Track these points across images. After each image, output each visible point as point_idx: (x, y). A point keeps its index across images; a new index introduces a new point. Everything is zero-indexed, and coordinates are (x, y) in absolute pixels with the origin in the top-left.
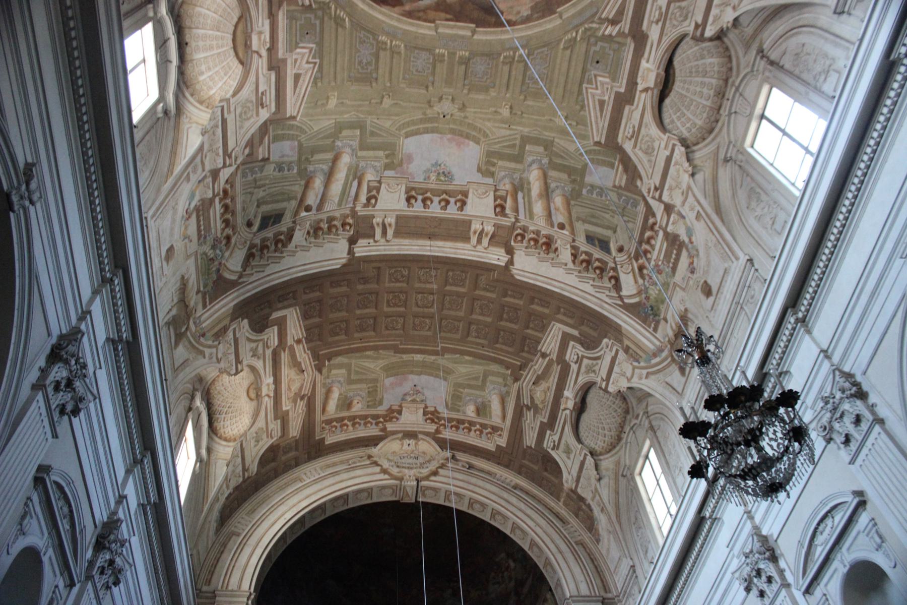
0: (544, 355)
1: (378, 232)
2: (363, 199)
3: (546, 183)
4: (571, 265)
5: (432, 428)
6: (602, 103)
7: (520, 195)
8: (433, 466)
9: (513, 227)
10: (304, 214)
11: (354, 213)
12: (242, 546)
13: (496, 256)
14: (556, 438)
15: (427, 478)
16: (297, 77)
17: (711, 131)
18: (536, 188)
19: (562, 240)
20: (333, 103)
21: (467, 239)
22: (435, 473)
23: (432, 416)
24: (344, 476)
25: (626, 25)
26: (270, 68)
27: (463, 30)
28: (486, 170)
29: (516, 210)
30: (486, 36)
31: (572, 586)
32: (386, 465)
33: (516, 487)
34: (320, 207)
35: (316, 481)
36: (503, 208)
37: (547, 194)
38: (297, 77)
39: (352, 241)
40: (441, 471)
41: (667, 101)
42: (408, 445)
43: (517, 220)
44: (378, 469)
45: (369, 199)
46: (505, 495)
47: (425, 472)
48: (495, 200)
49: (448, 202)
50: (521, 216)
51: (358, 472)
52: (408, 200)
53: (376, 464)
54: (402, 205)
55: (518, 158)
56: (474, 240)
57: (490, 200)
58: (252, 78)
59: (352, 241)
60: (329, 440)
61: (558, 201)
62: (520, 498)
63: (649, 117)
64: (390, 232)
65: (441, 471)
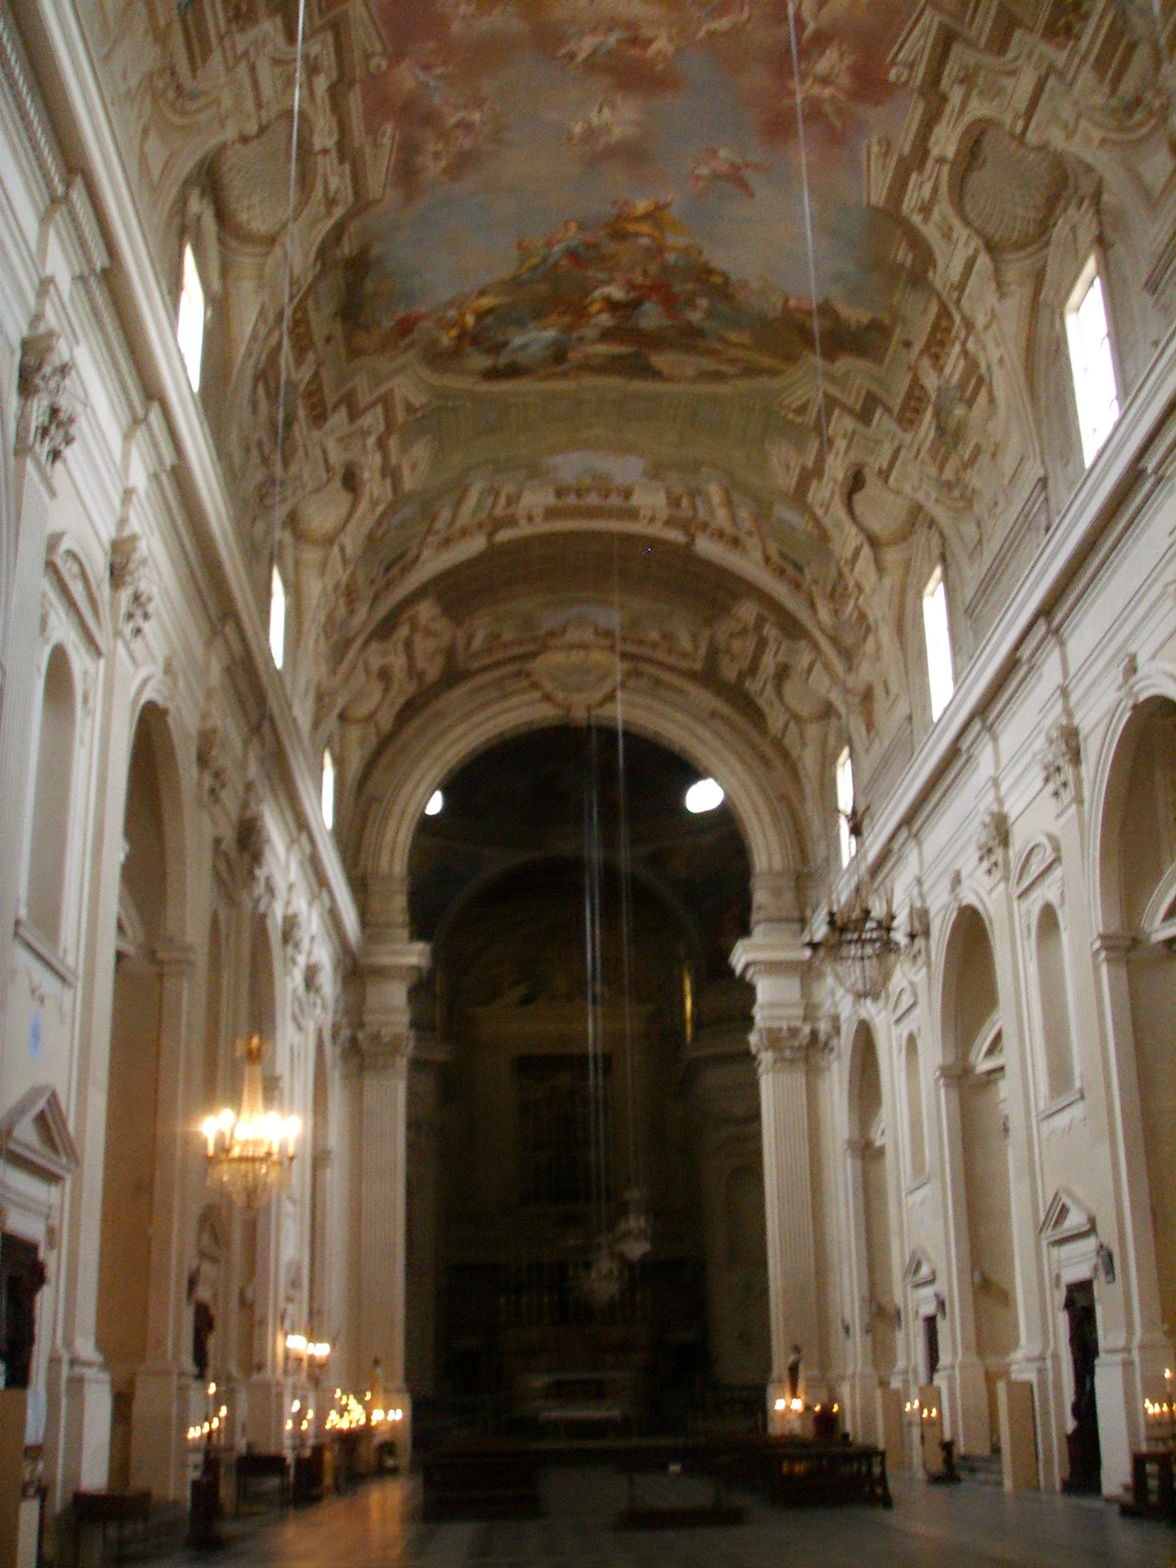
1: (523, 522)
4: (761, 562)
8: (606, 687)
12: (386, 817)
13: (675, 536)
15: (601, 704)
17: (904, 539)
19: (752, 543)
23: (608, 634)
24: (496, 708)
25: (811, 417)
26: (384, 476)
27: (615, 382)
28: (656, 472)
29: (695, 508)
31: (764, 858)
32: (549, 686)
33: (714, 714)
35: (460, 720)
37: (729, 503)
38: (413, 467)
39: (491, 535)
41: (858, 498)
42: (575, 657)
43: (695, 517)
44: (537, 695)
45: (509, 504)
47: (598, 695)
48: (668, 497)
49: (607, 496)
51: (515, 701)
52: (559, 494)
54: (550, 499)
56: (646, 521)
60: (475, 665)
61: (744, 514)
62: (717, 734)
64: (538, 520)
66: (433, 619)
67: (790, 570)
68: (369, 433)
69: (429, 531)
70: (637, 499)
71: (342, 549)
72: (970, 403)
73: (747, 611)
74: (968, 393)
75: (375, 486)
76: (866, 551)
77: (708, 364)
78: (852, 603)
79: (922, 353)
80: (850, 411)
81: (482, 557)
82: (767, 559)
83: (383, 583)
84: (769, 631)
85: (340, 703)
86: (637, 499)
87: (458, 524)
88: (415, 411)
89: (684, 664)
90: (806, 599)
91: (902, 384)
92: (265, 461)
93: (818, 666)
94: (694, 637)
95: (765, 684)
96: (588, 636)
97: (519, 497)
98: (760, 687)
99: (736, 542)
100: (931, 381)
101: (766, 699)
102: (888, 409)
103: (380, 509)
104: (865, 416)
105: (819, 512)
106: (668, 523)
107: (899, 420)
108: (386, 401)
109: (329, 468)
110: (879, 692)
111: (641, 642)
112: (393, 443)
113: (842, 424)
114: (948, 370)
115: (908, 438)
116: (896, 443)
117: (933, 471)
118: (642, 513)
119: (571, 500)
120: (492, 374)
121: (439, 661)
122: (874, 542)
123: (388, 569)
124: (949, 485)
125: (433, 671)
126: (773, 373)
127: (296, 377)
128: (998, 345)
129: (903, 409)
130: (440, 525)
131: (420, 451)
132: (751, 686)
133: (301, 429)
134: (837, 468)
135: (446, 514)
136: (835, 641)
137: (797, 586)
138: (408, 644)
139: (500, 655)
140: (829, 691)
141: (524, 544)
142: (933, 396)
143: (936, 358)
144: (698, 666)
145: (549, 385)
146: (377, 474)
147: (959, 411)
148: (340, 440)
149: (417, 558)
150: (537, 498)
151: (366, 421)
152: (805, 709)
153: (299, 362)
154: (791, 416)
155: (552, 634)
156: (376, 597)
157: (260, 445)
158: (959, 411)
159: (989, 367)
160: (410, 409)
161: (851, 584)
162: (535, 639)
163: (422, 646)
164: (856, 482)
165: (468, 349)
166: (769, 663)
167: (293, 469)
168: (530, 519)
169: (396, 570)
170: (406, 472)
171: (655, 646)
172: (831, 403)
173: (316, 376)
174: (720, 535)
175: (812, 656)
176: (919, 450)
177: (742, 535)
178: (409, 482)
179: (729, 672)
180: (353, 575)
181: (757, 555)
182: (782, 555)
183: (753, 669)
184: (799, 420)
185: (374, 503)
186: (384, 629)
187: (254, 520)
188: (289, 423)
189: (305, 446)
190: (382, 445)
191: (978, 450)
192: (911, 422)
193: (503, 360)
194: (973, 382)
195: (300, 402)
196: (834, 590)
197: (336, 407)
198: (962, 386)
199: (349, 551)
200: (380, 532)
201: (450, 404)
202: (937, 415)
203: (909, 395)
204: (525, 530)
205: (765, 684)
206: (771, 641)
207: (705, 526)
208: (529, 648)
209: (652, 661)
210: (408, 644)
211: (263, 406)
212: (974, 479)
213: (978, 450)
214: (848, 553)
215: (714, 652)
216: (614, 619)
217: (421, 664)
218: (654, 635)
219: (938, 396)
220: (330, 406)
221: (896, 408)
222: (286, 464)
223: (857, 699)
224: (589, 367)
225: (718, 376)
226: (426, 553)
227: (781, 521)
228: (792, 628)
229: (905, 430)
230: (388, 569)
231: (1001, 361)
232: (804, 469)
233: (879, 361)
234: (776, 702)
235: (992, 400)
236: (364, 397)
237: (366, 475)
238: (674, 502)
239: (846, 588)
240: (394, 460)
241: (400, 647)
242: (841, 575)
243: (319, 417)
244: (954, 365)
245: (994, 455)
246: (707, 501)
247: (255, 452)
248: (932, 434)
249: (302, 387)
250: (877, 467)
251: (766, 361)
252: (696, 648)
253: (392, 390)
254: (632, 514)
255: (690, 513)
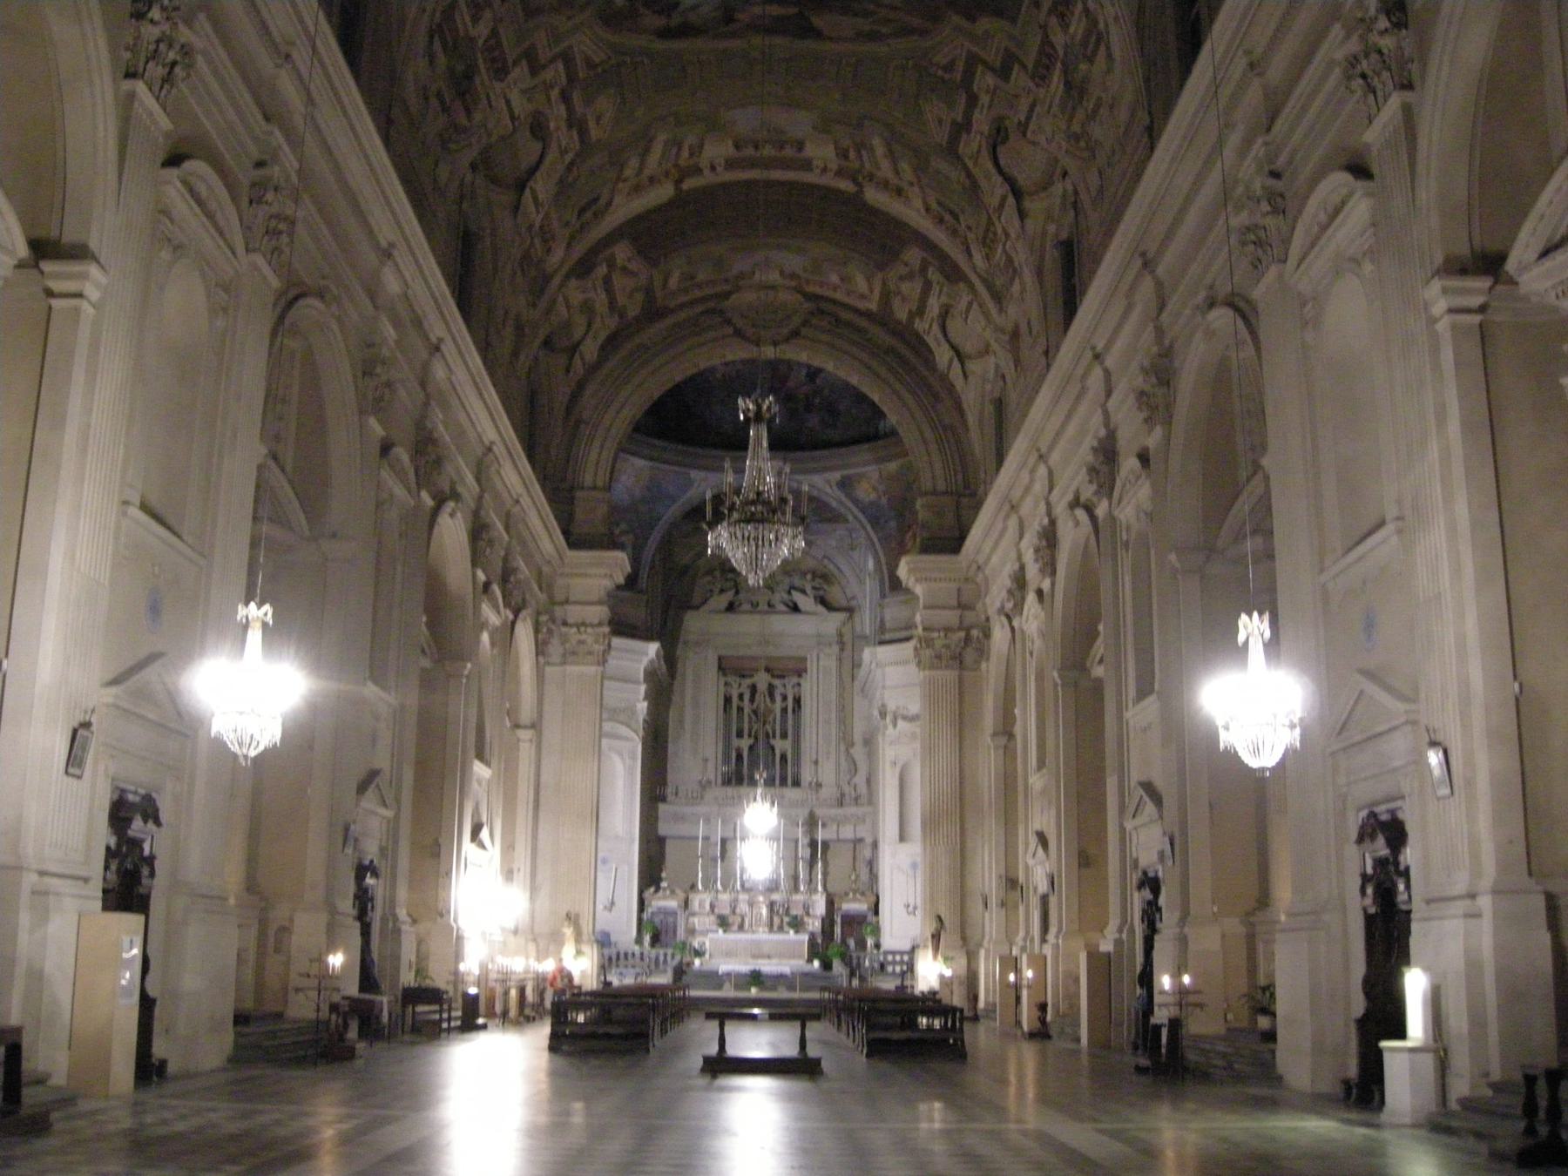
0: (906, 265)
1: (706, 172)
2: (685, 153)
3: (890, 150)
4: (923, 211)
5: (793, 284)
6: (940, 121)
7: (864, 152)
9: (859, 171)
10: (621, 185)
11: (676, 165)
14: (927, 326)
16: (598, 119)
17: (1045, 189)
18: (880, 150)
20: (639, 113)
21: (812, 170)
22: (795, 334)
23: (793, 276)
26: (570, 127)
30: (810, 44)
33: (890, 351)
34: (637, 175)
36: (846, 157)
37: (891, 154)
38: (598, 119)
39: (678, 182)
40: (804, 331)
43: (862, 166)
44: (730, 330)
45: (691, 155)
46: (875, 364)
48: (836, 148)
49: (782, 148)
50: (867, 165)
52: (737, 147)
53: (729, 322)
55: (860, 125)
56: (818, 171)
57: (832, 147)
58: (554, 145)
59: (678, 182)
61: (904, 166)
63: (985, 153)
64: (719, 169)
65: (804, 331)
66: (629, 260)
67: (947, 217)
68: (552, 87)
69: (619, 179)
70: (810, 150)
71: (533, 192)
72: (1091, 60)
73: (913, 255)
74: (1089, 52)
75: (563, 136)
76: (1011, 200)
77: (864, 25)
78: (1000, 250)
79: (1050, 12)
80: (992, 69)
81: (671, 204)
82: (928, 210)
83: (578, 226)
84: (933, 275)
85: (542, 334)
86: (810, 150)
87: (647, 172)
88: (596, 66)
89: (862, 305)
90: (962, 244)
91: (1034, 44)
92: (445, 109)
93: (975, 306)
94: (869, 279)
95: (931, 326)
96: (774, 277)
97: (701, 146)
98: (926, 326)
99: (899, 192)
100: (1059, 39)
101: (933, 338)
102: (1024, 67)
103: (568, 158)
104: (1004, 73)
105: (970, 164)
106: (840, 173)
107: (1032, 78)
108: (567, 58)
109: (513, 118)
110: (1024, 329)
111: (822, 285)
112: (576, 96)
113: (985, 81)
114: (1072, 30)
115: (1042, 91)
116: (1031, 99)
117: (1064, 127)
118: (815, 163)
119: (749, 151)
120: (665, 34)
121: (639, 297)
122: (1018, 194)
123: (582, 211)
124: (1077, 138)
125: (633, 311)
126: (923, 33)
127: (473, 32)
128: (1113, 5)
129: (1037, 63)
130: (628, 172)
131: (605, 104)
132: (920, 326)
133: (483, 76)
134: (982, 121)
135: (634, 163)
136: (984, 281)
137: (954, 233)
138: (607, 281)
139: (698, 293)
140: (984, 329)
141: (709, 192)
142: (1061, 52)
143: (1062, 16)
144: (873, 306)
145: (722, 44)
146: (563, 125)
147: (1083, 67)
148: (524, 92)
149: (609, 204)
150: (717, 150)
151: (548, 75)
152: (968, 347)
153: (476, 19)
154: (940, 73)
155: (741, 276)
156: (572, 238)
157: (439, 95)
158: (1083, 67)
159: (1107, 25)
160: (590, 65)
161: (999, 231)
162: (726, 281)
163: (619, 281)
164: (998, 136)
165: (642, 10)
166: (934, 305)
167: (478, 117)
168: (713, 168)
169: (588, 215)
170: (592, 124)
171: (835, 289)
172: (973, 61)
173: (494, 33)
174: (885, 185)
175: (970, 297)
176: (1050, 107)
177: (905, 186)
178: (595, 133)
179: (901, 313)
180: (547, 216)
181: (918, 203)
182: (940, 204)
183: (921, 311)
184: (947, 76)
185: (564, 152)
186: (583, 268)
187: (436, 165)
188: (469, 75)
189: (488, 95)
190: (565, 98)
191: (1098, 106)
192: (1043, 78)
193: (676, 20)
194: (1093, 39)
195: (479, 55)
196: (985, 238)
197: (515, 63)
198: (1085, 43)
199: (541, 197)
200: (570, 179)
201: (628, 60)
202: (1065, 72)
203: (1041, 52)
204: (707, 178)
205: (931, 326)
206: (934, 285)
207: (871, 177)
208: (727, 288)
209: (834, 302)
210: (607, 281)
211: (442, 60)
212: (1097, 131)
213: (1098, 106)
214: (995, 202)
215: (886, 297)
216: (794, 262)
217: (621, 300)
218: (834, 278)
219: (1066, 54)
220: (510, 62)
221: (1030, 66)
222: (468, 111)
223: (1007, 338)
224: (756, 27)
225: (873, 37)
226: (618, 200)
227: (938, 172)
228: (953, 274)
229: (1037, 85)
230: (582, 211)
231: (1116, 19)
232: (954, 123)
233: (1014, 21)
234: (942, 340)
235: (1110, 56)
236: (544, 54)
237: (552, 125)
238: (843, 154)
239: (995, 234)
240: (579, 109)
241: (599, 283)
242: (990, 222)
243: (501, 71)
244: (1077, 27)
245: (1112, 107)
246: (871, 150)
247: (434, 101)
248: (1062, 86)
249: (481, 42)
250: (1016, 121)
251: (916, 22)
252: (871, 291)
253: (571, 47)
254: (807, 165)
255: (857, 165)
